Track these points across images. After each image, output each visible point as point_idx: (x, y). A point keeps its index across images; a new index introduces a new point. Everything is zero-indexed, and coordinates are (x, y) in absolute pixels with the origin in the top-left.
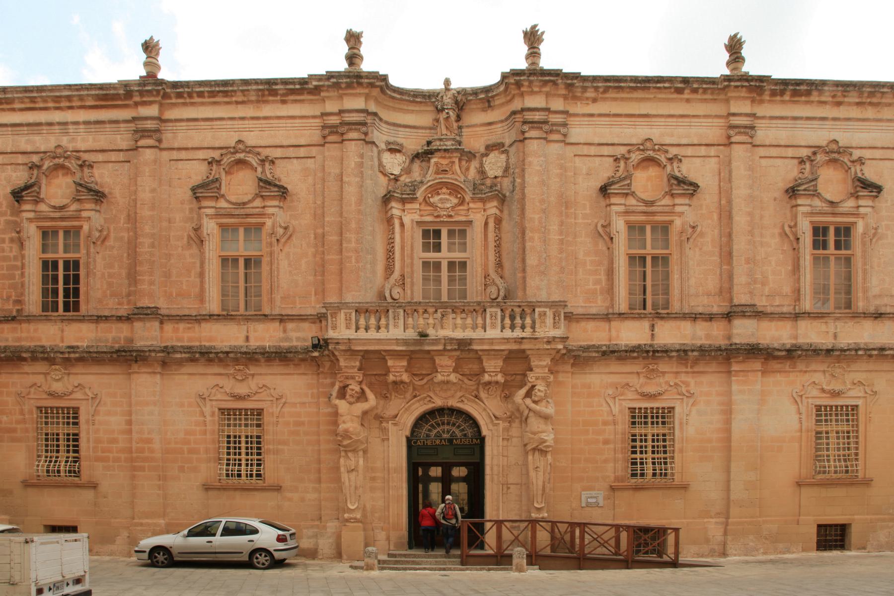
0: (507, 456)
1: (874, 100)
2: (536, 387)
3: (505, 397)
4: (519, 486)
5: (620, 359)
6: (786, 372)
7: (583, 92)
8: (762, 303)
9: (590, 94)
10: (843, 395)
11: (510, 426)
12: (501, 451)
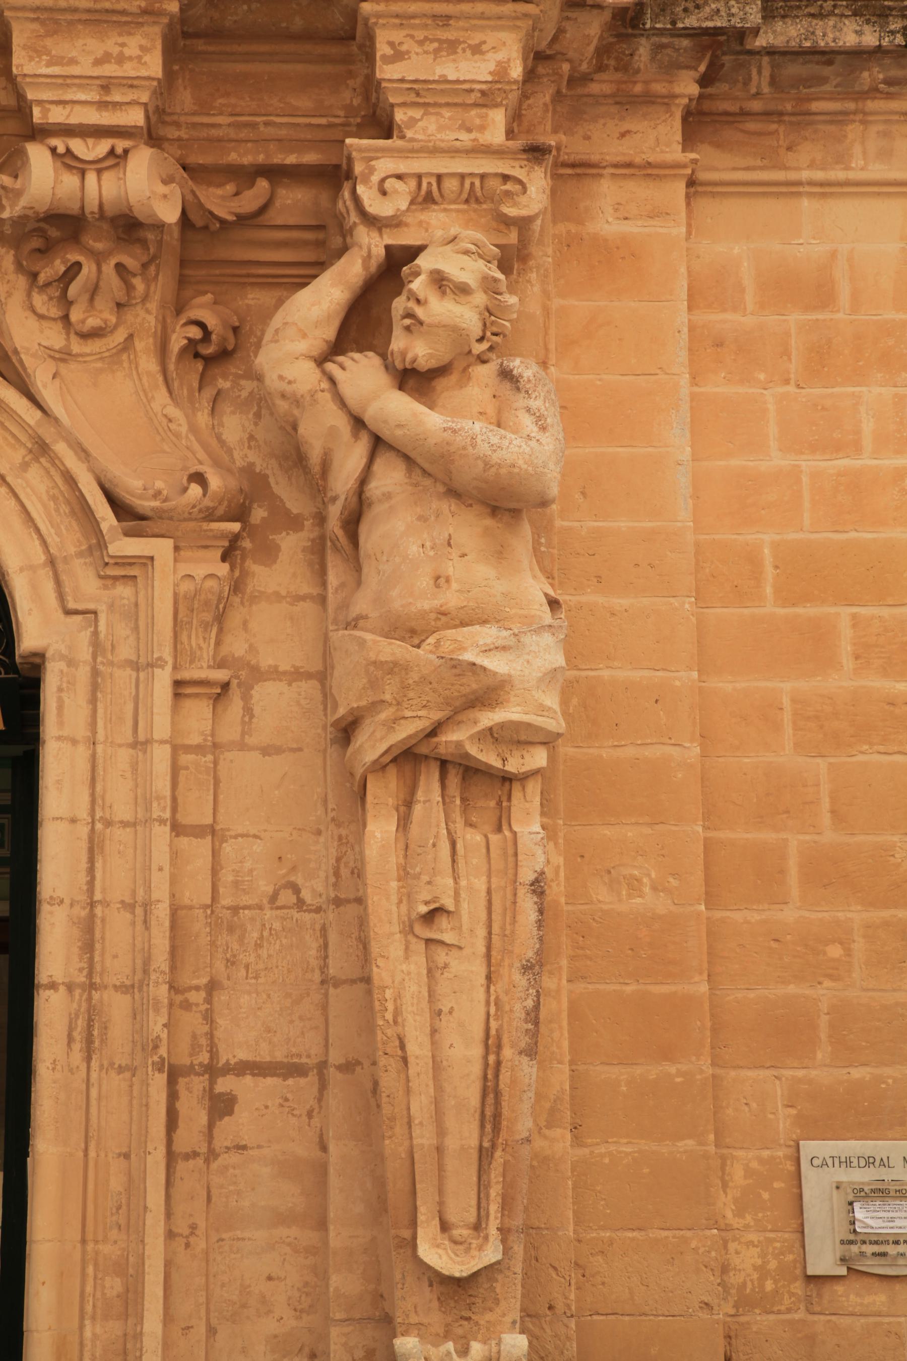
0: (211, 830)
2: (424, 262)
3: (192, 350)
4: (307, 1084)
11: (237, 587)
12: (163, 785)
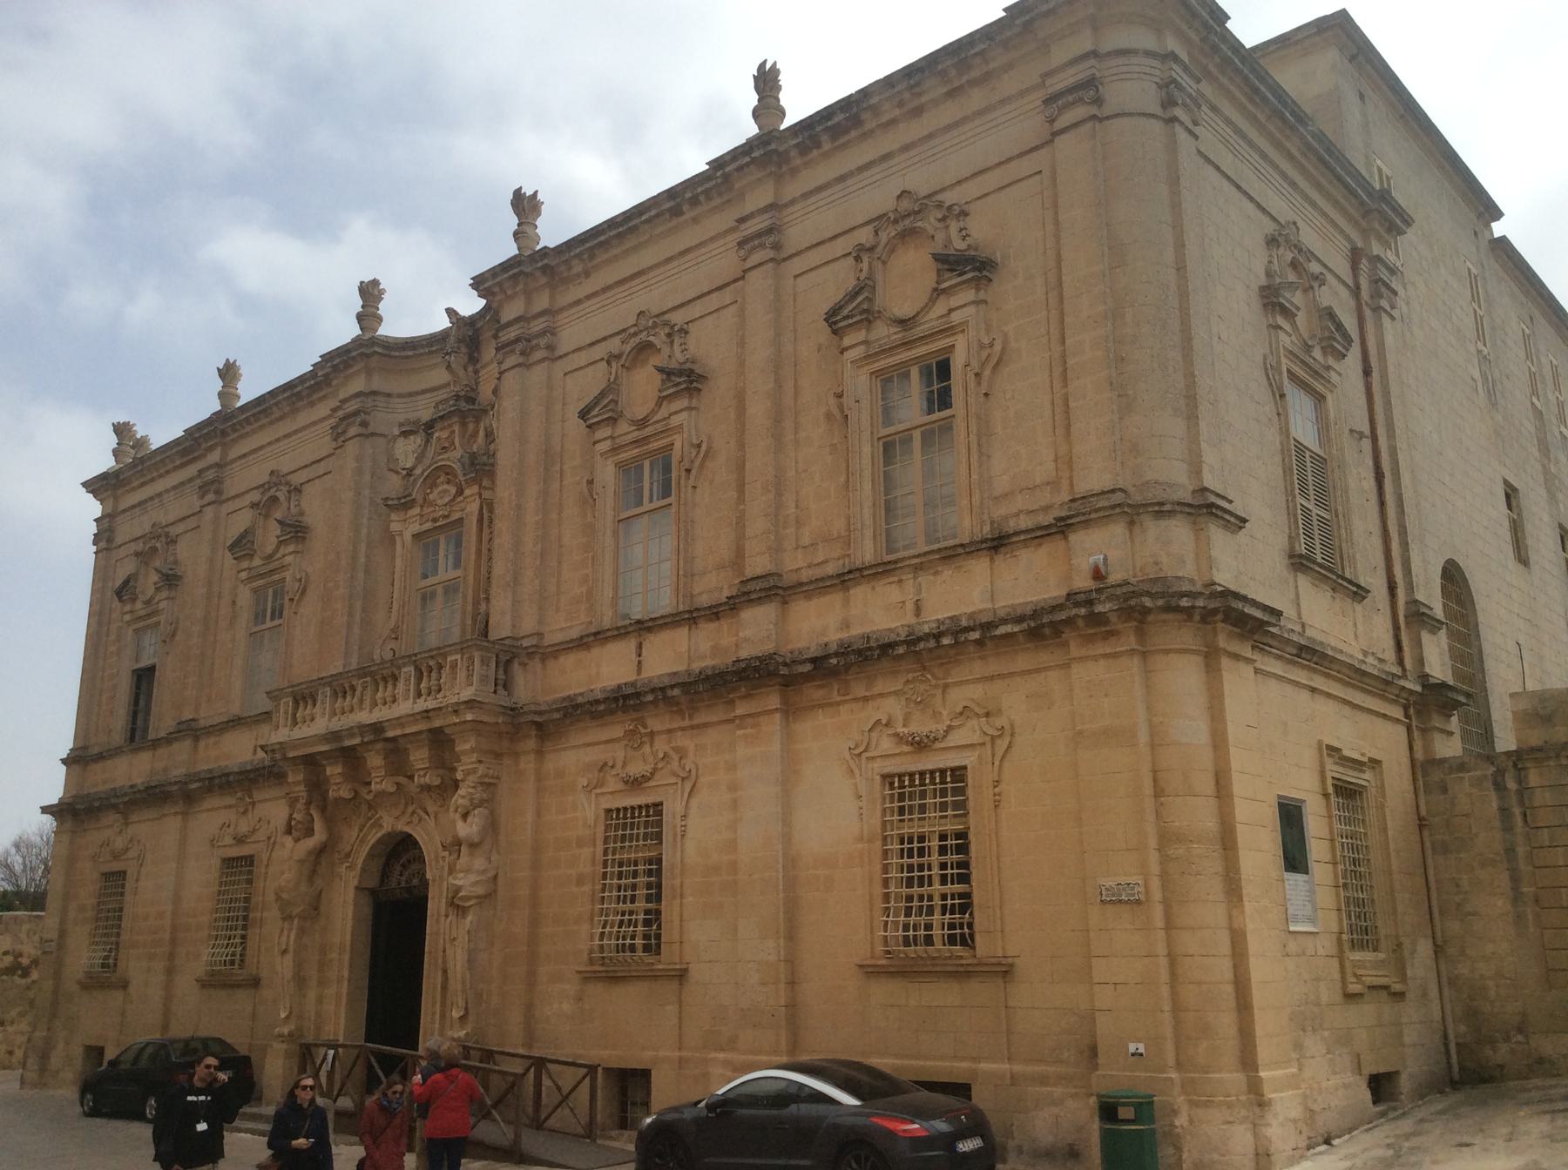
1: (975, 73)
5: (596, 716)
6: (830, 705)
7: (570, 269)
8: (795, 564)
9: (578, 268)
10: (938, 745)
